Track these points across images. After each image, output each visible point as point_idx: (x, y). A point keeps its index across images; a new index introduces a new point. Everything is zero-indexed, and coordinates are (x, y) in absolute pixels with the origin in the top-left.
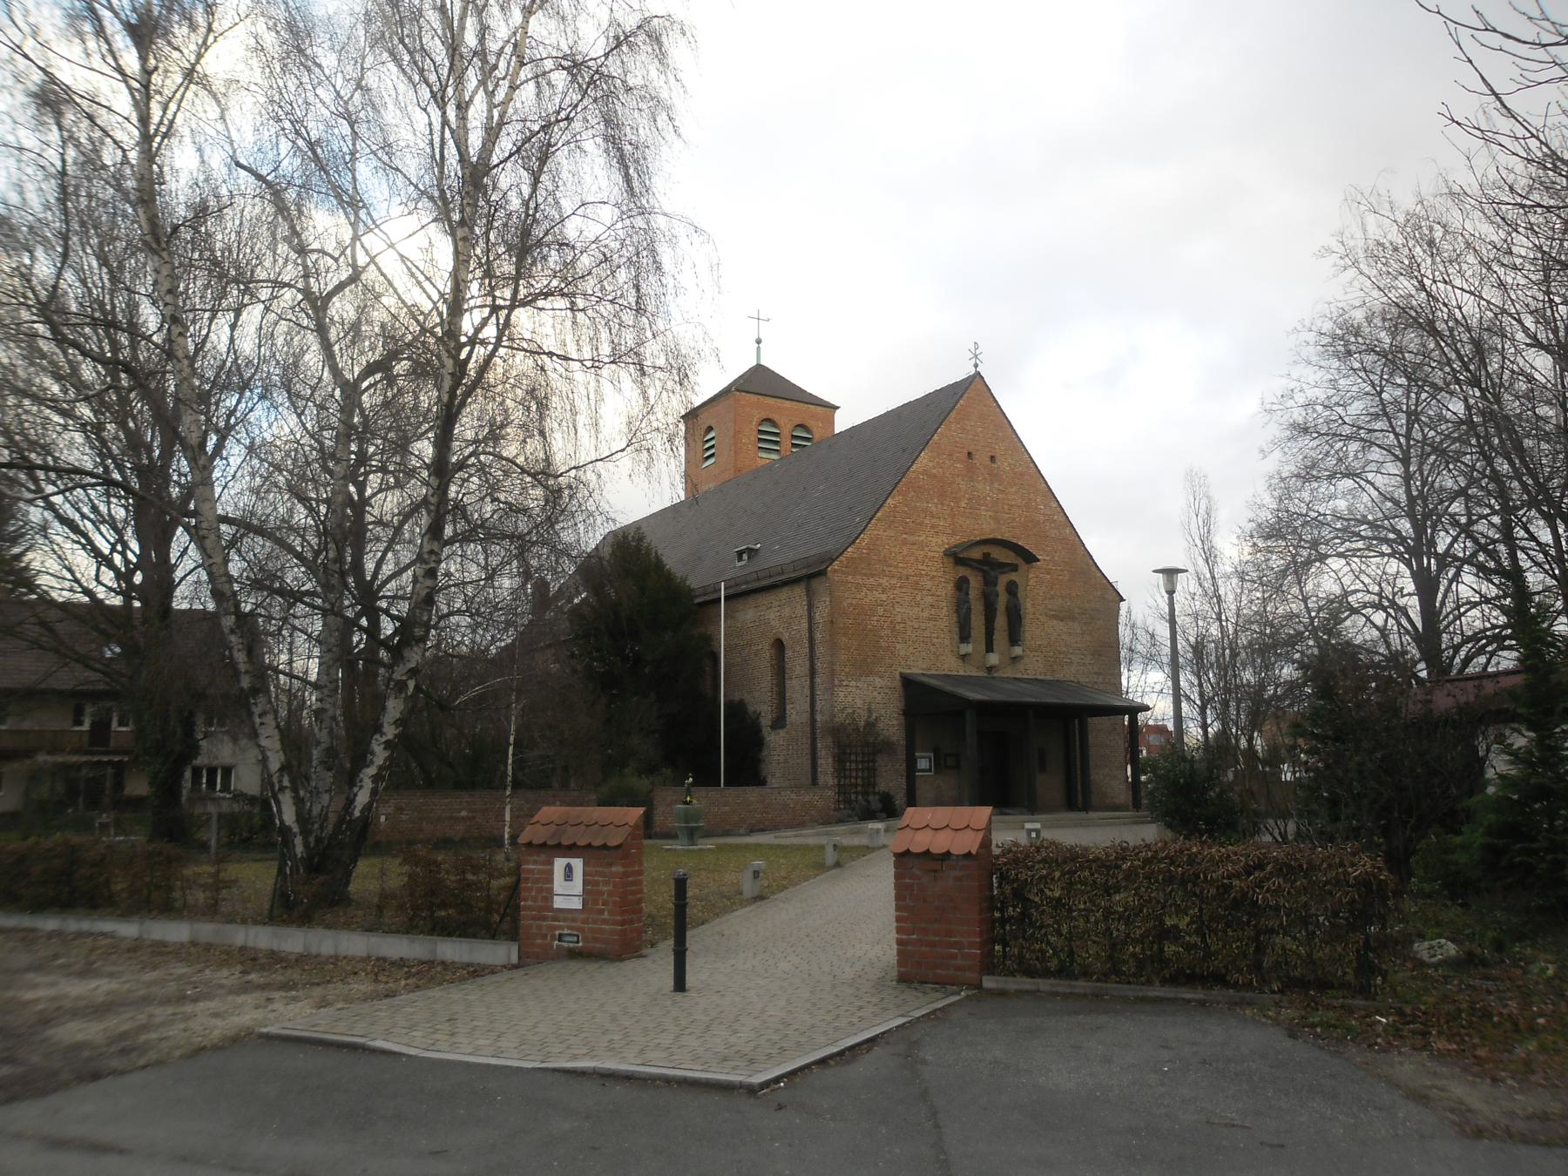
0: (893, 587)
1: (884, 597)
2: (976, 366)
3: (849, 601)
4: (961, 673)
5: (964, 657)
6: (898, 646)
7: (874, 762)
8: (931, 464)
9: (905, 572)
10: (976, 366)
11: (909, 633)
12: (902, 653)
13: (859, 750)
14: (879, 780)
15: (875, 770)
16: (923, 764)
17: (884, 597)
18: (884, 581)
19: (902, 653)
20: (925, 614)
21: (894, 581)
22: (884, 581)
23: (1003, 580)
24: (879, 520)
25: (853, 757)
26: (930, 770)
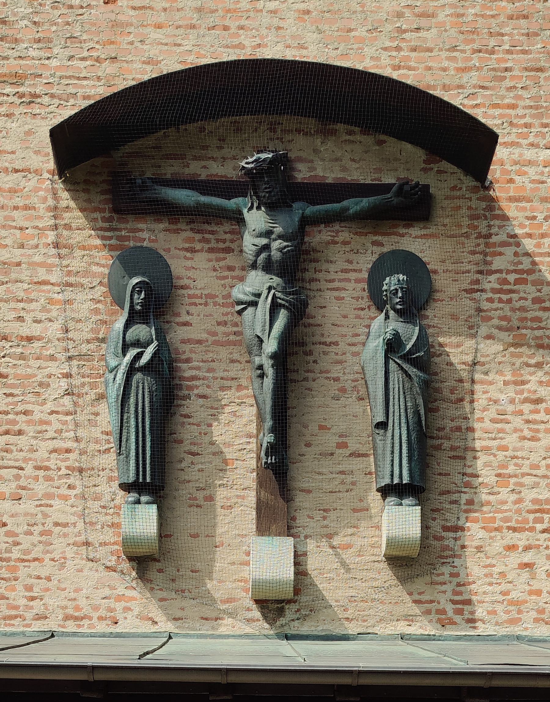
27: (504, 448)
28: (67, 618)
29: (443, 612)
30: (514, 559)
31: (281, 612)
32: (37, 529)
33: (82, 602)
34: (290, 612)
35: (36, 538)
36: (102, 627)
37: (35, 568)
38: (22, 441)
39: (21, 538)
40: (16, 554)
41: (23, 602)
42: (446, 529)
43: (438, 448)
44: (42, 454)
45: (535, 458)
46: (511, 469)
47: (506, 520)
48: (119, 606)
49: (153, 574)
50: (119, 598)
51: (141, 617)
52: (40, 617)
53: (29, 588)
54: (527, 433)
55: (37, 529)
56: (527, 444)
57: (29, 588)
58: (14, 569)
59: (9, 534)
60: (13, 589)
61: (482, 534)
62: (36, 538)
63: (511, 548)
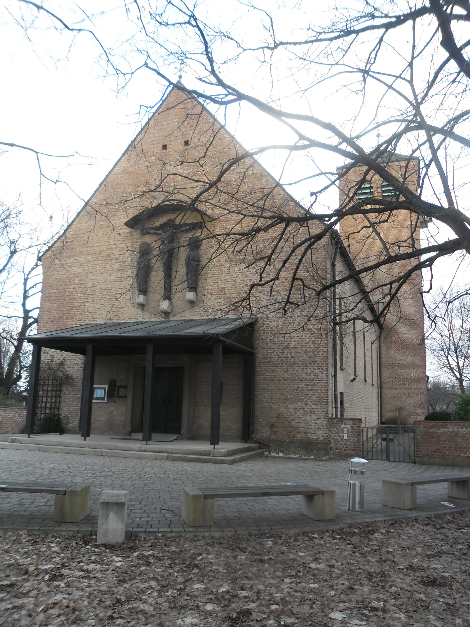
0: (89, 262)
1: (80, 270)
2: (180, 77)
3: (55, 277)
4: (140, 320)
5: (142, 306)
6: (88, 304)
7: (60, 391)
8: (128, 164)
9: (99, 249)
10: (180, 77)
11: (97, 294)
12: (90, 309)
13: (50, 382)
14: (62, 405)
15: (60, 397)
16: (99, 393)
17: (80, 270)
18: (81, 259)
19: (90, 309)
20: (113, 277)
21: (89, 258)
22: (81, 259)
23: (185, 238)
24: (83, 216)
25: (45, 388)
26: (103, 399)
27: (215, 277)
28: (129, 319)
29: (201, 314)
30: (216, 301)
31: (169, 316)
32: (124, 301)
33: (132, 315)
34: (171, 315)
35: (124, 303)
36: (135, 321)
37: (124, 309)
38: (123, 283)
39: (122, 303)
40: (120, 306)
41: (121, 316)
42: (202, 295)
43: (202, 278)
44: (126, 285)
45: (222, 278)
46: (217, 281)
47: (215, 292)
48: (138, 316)
49: (145, 309)
50: (138, 314)
51: (142, 318)
52: (123, 319)
53: (122, 313)
54: (220, 273)
55: (124, 301)
56: (220, 275)
57: (122, 313)
58: (119, 309)
59: (120, 302)
60: (119, 313)
61: (210, 296)
62: (124, 303)
63: (216, 299)
